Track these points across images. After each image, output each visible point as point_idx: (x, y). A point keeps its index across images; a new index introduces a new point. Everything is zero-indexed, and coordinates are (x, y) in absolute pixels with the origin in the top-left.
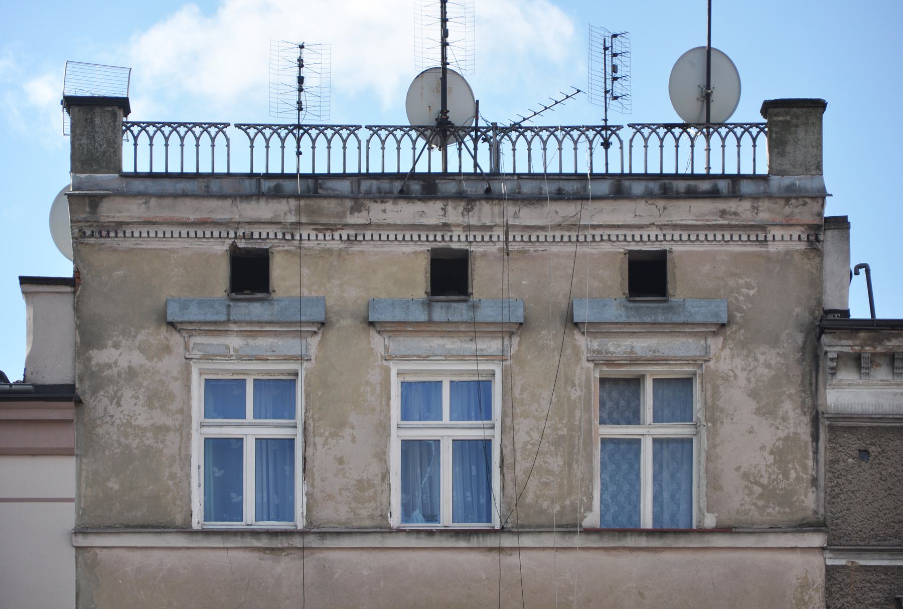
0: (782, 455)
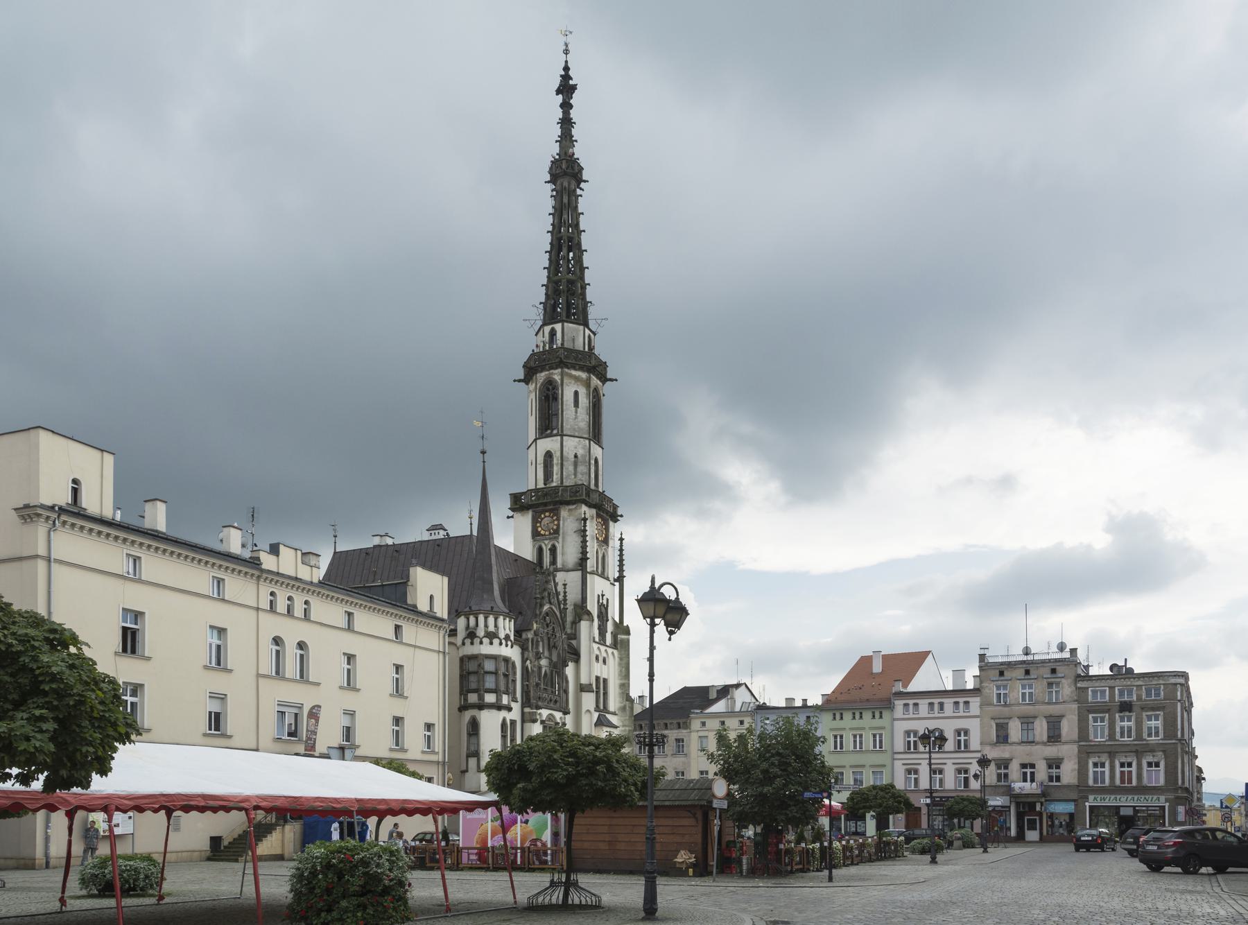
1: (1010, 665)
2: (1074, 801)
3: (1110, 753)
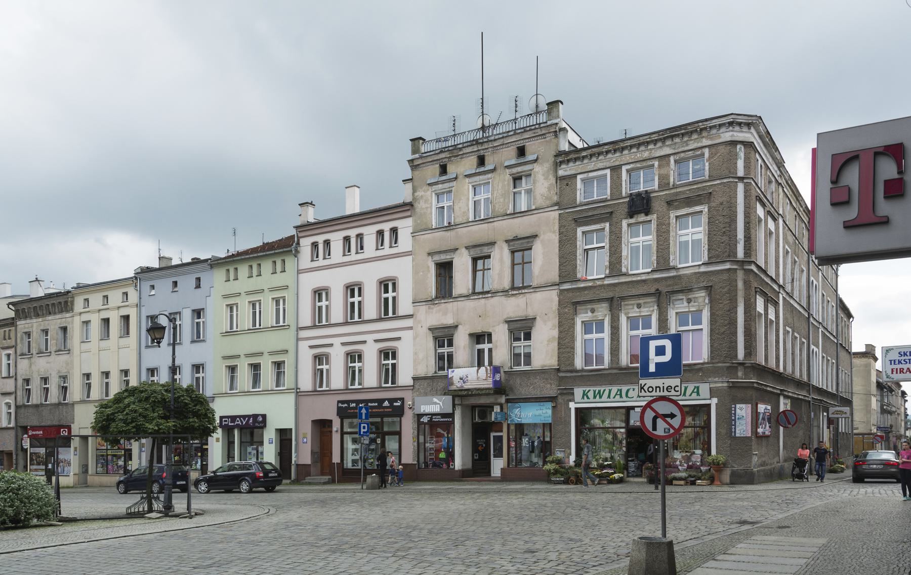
0: (549, 189)
1: (455, 152)
2: (552, 399)
3: (611, 300)
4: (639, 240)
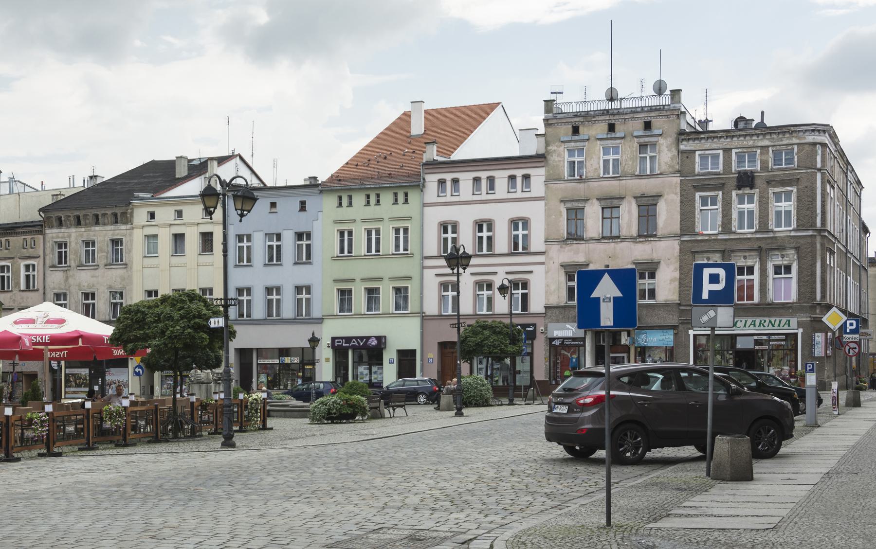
1: (588, 117)
2: (674, 327)
4: (744, 206)
